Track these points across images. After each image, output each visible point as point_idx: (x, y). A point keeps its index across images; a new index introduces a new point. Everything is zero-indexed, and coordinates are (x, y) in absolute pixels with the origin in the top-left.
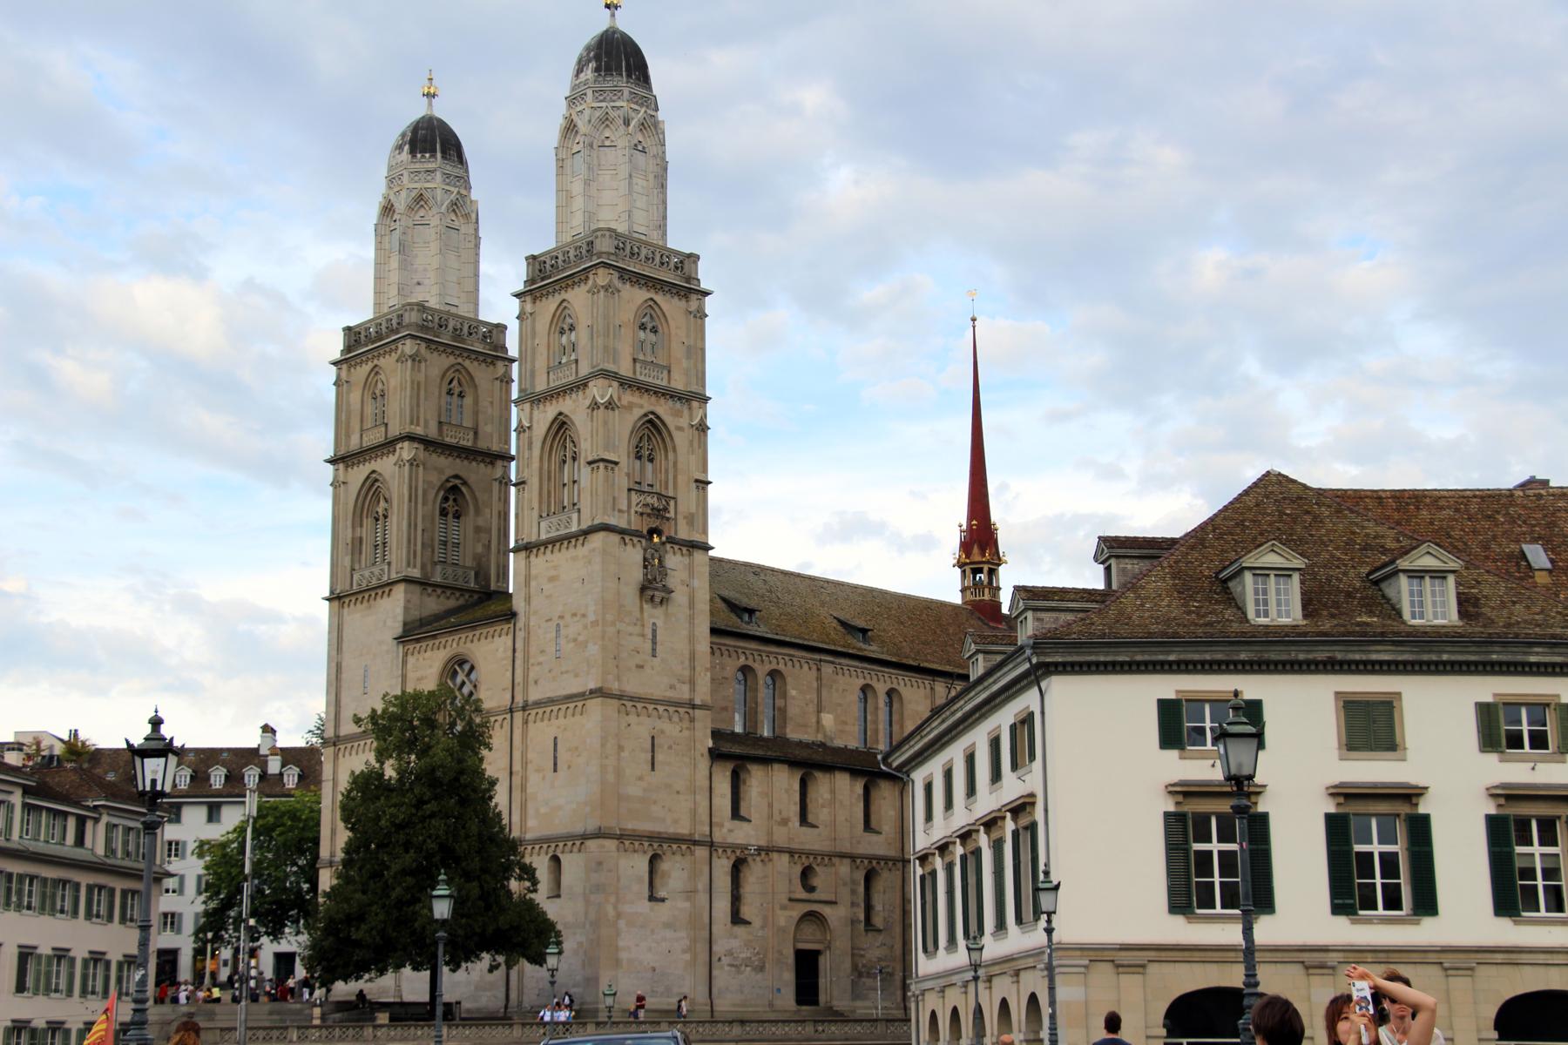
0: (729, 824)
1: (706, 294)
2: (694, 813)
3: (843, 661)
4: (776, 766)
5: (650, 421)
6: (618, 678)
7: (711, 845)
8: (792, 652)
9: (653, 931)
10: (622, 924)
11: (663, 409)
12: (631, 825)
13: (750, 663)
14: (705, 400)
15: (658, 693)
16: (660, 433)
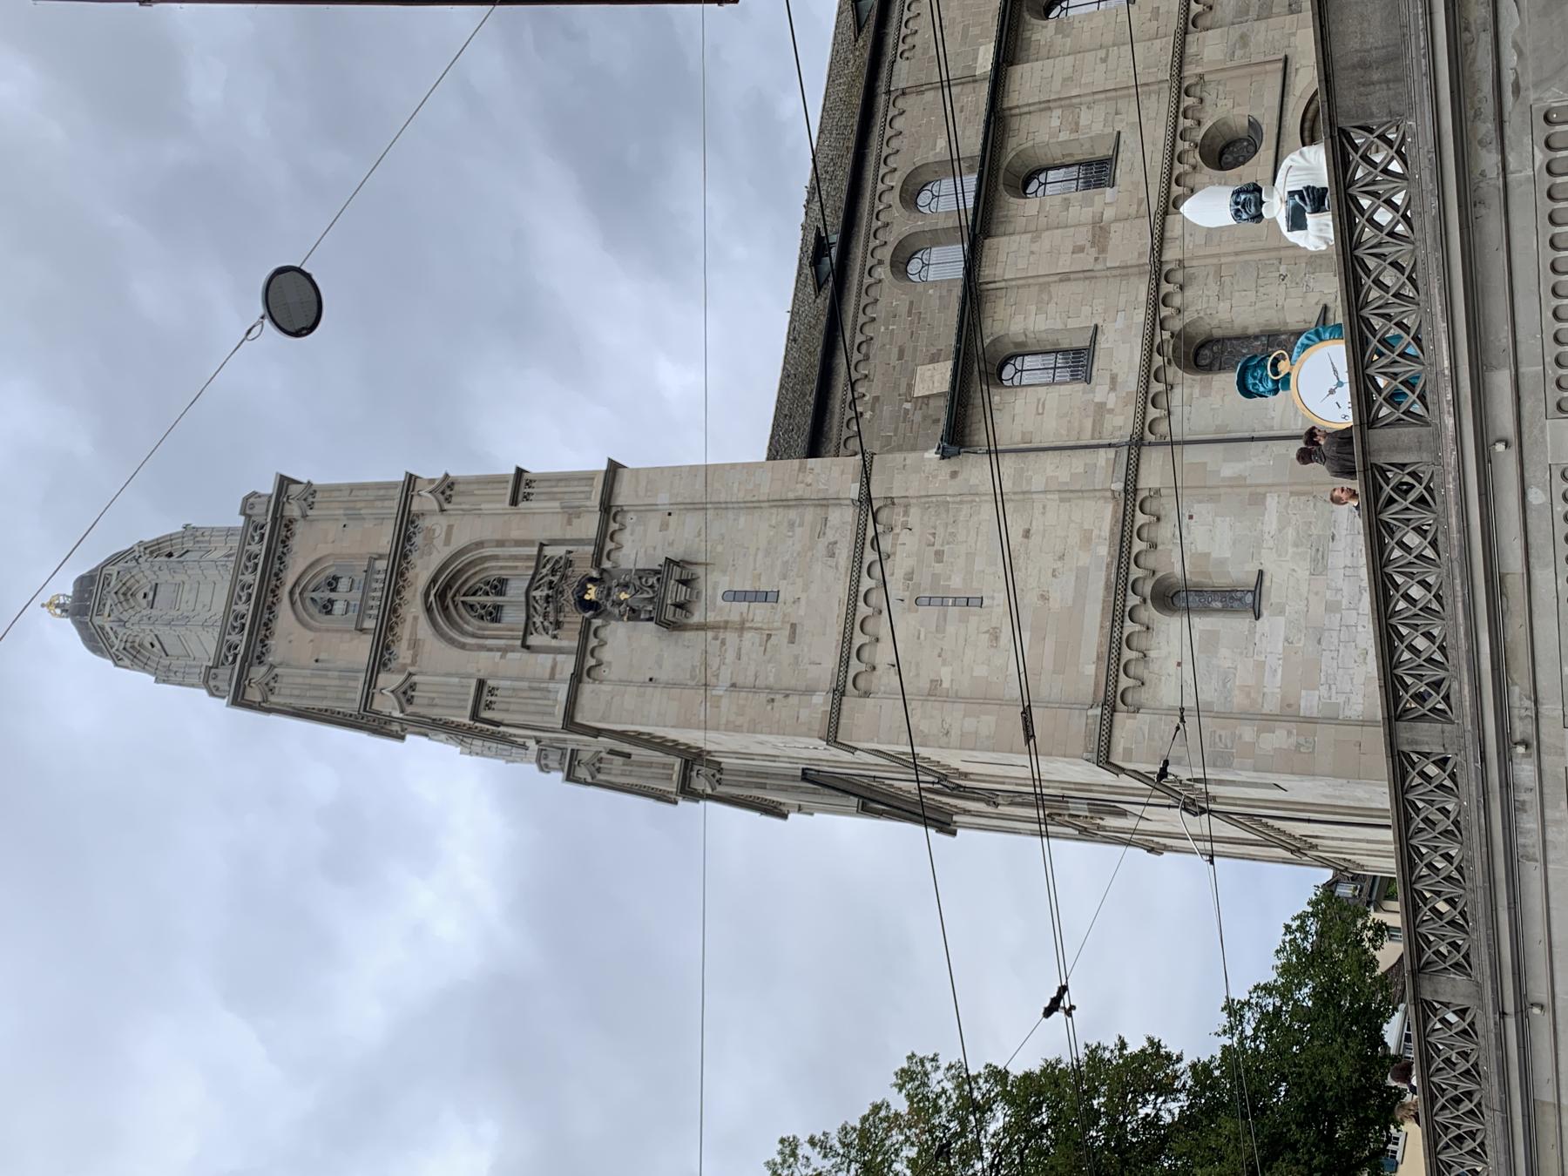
0: (1100, 391)
1: (284, 482)
2: (1068, 494)
3: (891, 41)
4: (987, 272)
5: (441, 596)
6: (809, 691)
7: (1137, 444)
8: (871, 160)
9: (1332, 607)
10: (1309, 703)
11: (422, 571)
12: (1088, 671)
13: (886, 254)
14: (411, 479)
15: (841, 590)
16: (460, 572)
